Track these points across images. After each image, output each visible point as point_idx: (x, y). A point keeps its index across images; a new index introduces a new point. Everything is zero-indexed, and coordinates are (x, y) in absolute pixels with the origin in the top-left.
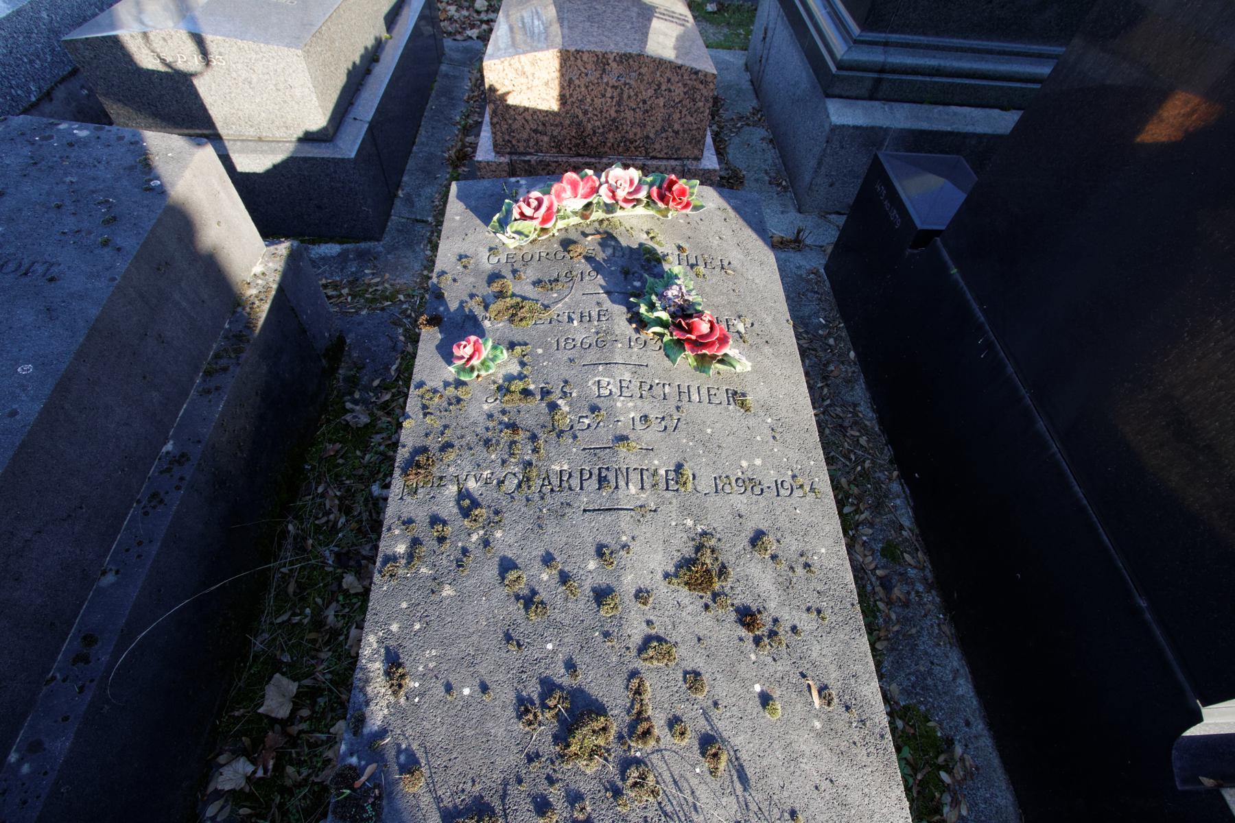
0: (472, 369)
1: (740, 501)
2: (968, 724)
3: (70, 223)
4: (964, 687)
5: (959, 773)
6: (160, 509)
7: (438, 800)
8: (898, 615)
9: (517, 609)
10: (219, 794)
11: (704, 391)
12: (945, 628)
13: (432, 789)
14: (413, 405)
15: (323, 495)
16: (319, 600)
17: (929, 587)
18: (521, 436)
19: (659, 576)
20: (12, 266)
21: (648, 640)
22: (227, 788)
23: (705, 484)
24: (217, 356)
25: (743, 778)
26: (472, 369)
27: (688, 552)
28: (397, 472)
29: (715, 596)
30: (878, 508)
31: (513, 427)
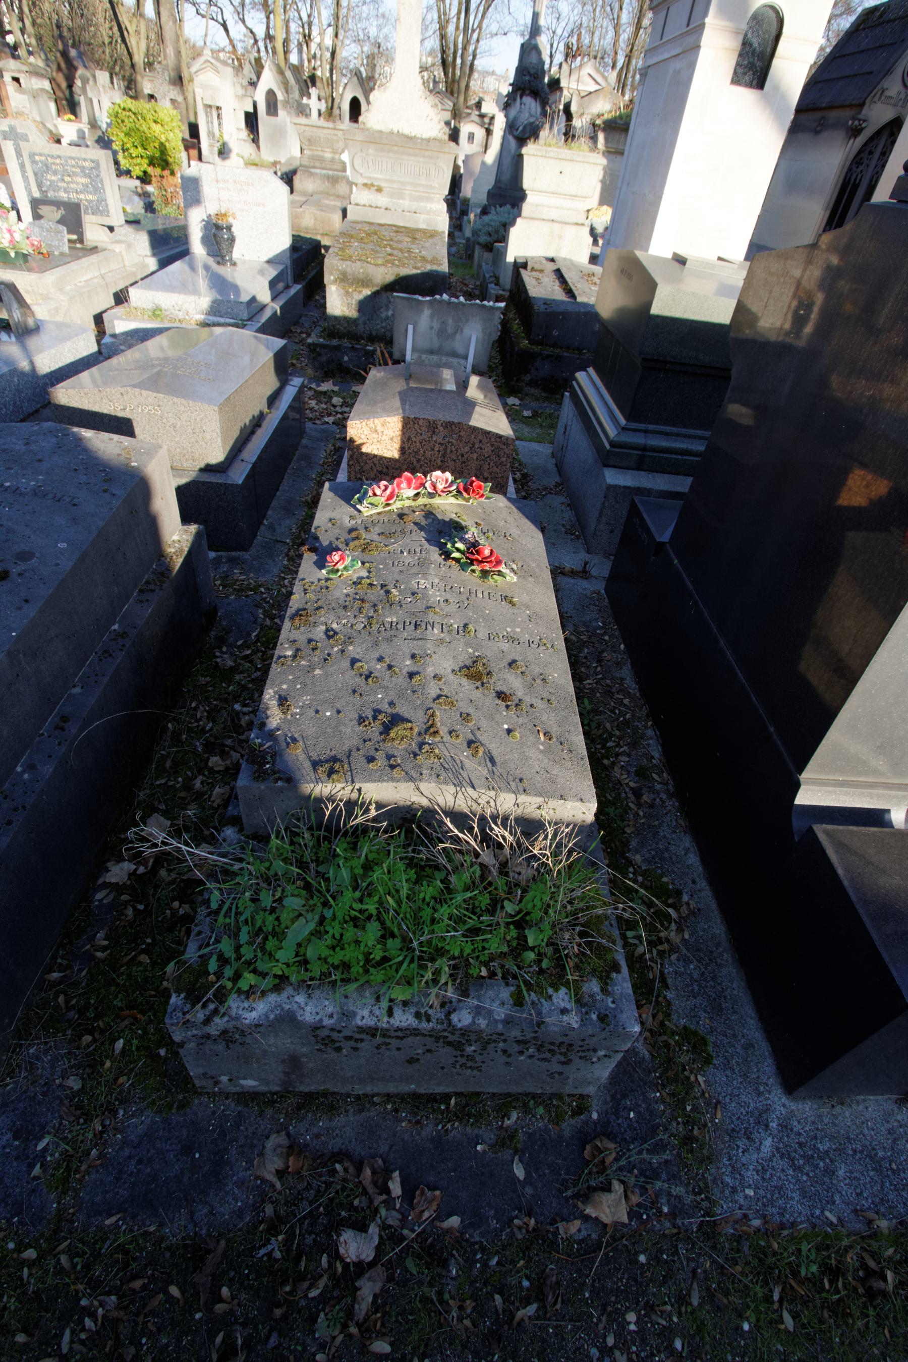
0: (338, 571)
1: (505, 646)
2: (694, 882)
3: (83, 479)
4: (693, 859)
5: (684, 910)
6: (109, 659)
7: (309, 757)
8: (645, 813)
9: (360, 681)
10: (106, 885)
11: (486, 594)
12: (681, 822)
13: (306, 751)
14: (297, 588)
15: (195, 709)
16: (189, 773)
17: (670, 796)
18: (366, 605)
19: (449, 670)
20: (50, 496)
21: (439, 697)
22: (113, 880)
23: (483, 634)
24: (148, 583)
25: (492, 761)
26: (338, 571)
27: (468, 663)
28: (287, 620)
29: (483, 684)
30: (634, 745)
31: (363, 600)
